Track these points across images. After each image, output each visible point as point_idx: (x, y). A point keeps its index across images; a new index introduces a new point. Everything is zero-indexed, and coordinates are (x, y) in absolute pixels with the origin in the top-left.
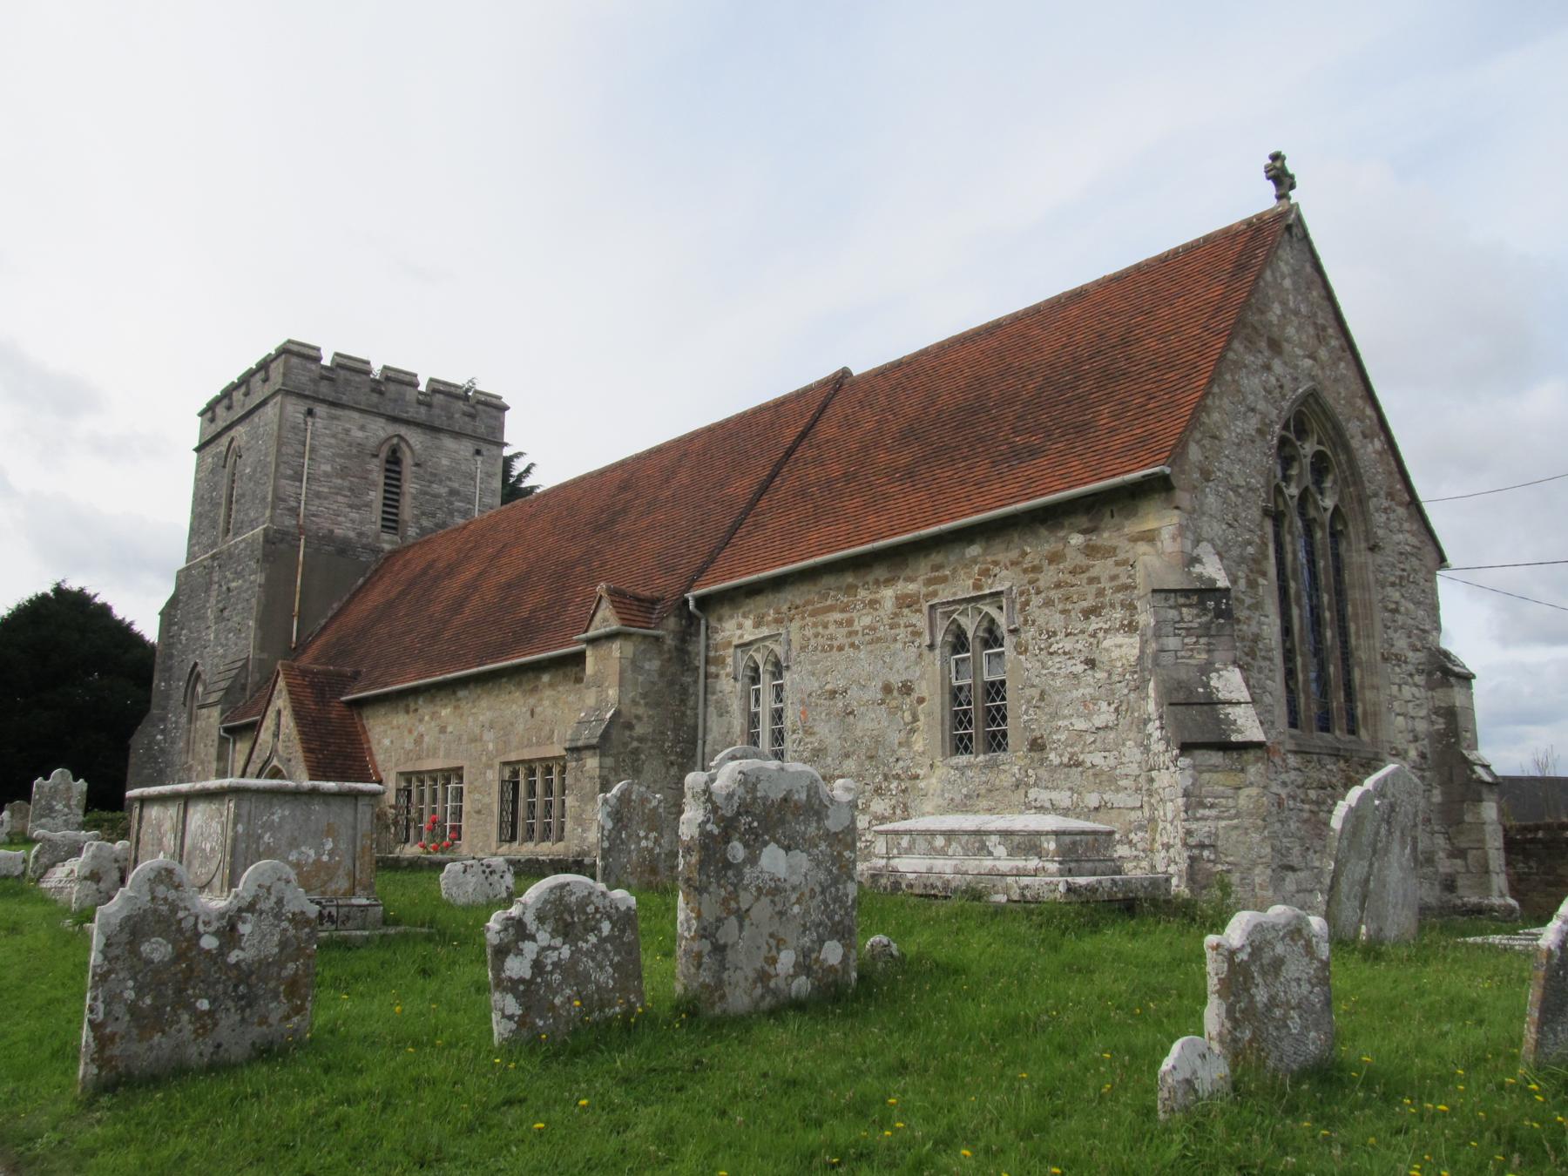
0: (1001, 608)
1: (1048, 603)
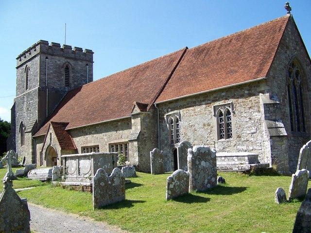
0: (230, 107)
1: (241, 106)
